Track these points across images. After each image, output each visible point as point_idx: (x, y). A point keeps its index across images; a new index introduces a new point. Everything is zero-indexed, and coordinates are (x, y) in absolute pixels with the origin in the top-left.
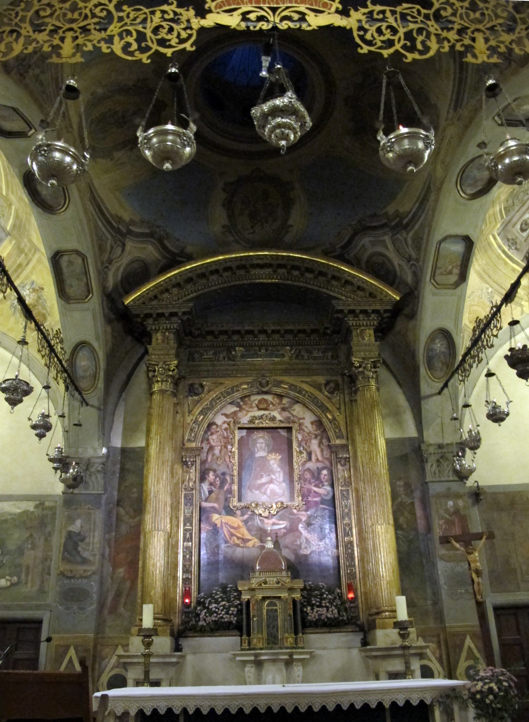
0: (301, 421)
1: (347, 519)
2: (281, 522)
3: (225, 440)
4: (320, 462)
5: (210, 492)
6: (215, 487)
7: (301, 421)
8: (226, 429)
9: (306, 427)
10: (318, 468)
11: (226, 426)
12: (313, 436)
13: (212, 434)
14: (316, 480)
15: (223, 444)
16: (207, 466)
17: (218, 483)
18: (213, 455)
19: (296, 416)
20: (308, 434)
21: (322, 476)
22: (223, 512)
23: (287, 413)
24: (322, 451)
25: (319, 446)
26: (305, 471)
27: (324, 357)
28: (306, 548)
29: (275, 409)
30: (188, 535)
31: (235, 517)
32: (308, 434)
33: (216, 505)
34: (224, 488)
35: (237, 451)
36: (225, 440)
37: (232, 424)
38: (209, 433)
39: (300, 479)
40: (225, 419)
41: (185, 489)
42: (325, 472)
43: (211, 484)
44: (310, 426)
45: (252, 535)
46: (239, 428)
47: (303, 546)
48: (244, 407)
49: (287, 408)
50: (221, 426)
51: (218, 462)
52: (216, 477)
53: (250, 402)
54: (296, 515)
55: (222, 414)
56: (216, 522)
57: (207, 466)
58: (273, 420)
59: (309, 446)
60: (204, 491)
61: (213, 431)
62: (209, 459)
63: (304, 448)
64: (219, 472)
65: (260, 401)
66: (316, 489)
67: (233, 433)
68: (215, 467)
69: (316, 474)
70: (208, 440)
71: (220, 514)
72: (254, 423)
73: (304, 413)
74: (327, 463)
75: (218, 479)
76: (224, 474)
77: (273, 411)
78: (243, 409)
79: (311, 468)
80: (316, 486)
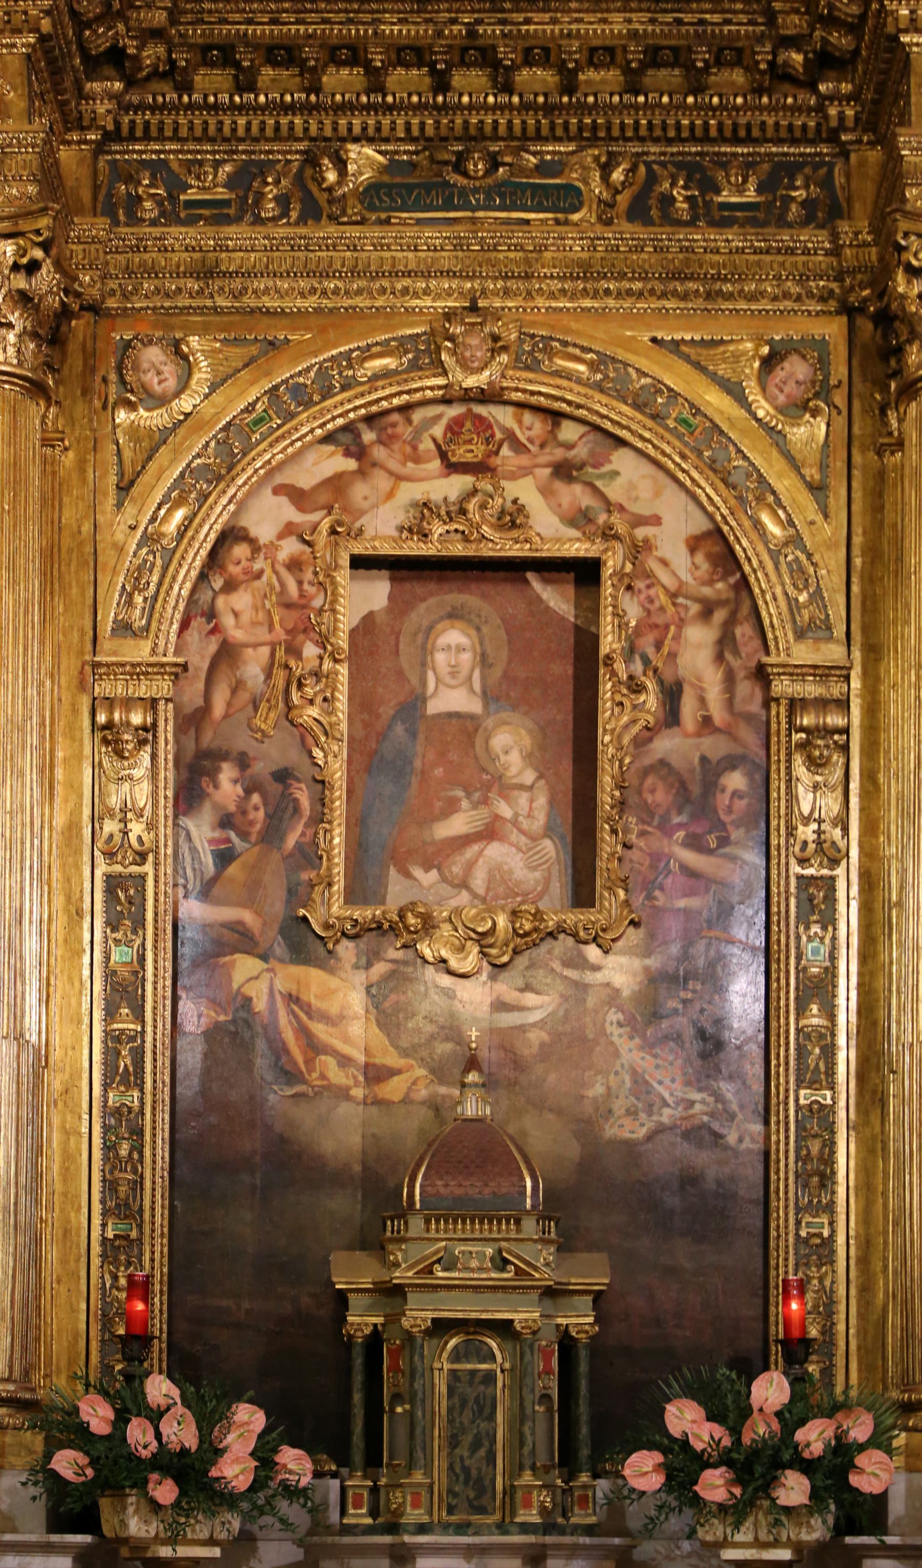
0: (641, 533)
1: (815, 1008)
2: (530, 999)
3: (292, 618)
4: (717, 730)
5: (224, 857)
6: (244, 835)
7: (641, 533)
8: (294, 565)
9: (664, 563)
10: (704, 760)
11: (290, 547)
12: (695, 608)
13: (230, 586)
14: (694, 817)
15: (280, 633)
16: (207, 738)
17: (261, 814)
18: (237, 687)
19: (622, 508)
20: (673, 596)
21: (723, 800)
22: (280, 949)
23: (578, 488)
24: (730, 680)
25: (719, 658)
26: (646, 772)
27: (769, 205)
28: (632, 1113)
29: (525, 472)
30: (125, 1061)
31: (332, 971)
32: (673, 596)
33: (247, 917)
34: (282, 839)
35: (343, 670)
36: (292, 618)
37: (322, 537)
38: (218, 583)
39: (621, 805)
40: (290, 513)
41: (110, 855)
42: (735, 780)
43: (225, 822)
44: (680, 559)
45: (405, 1053)
46: (359, 563)
47: (619, 1106)
48: (379, 453)
49: (581, 467)
50: (273, 547)
51: (258, 722)
52: (248, 792)
53: (406, 432)
54: (596, 968)
55: (276, 491)
56: (250, 990)
57: (207, 738)
58: (514, 525)
59: (673, 656)
60: (193, 850)
61: (233, 569)
62: (219, 708)
63: (646, 661)
64: (260, 768)
65: (454, 428)
66: (689, 857)
67: (327, 584)
68: (242, 742)
69: (696, 790)
70: (211, 614)
71: (264, 958)
72: (425, 536)
73: (657, 494)
74: (750, 738)
75: (256, 798)
76: (283, 776)
77: (513, 477)
78: (374, 465)
79: (676, 762)
80: (695, 843)
